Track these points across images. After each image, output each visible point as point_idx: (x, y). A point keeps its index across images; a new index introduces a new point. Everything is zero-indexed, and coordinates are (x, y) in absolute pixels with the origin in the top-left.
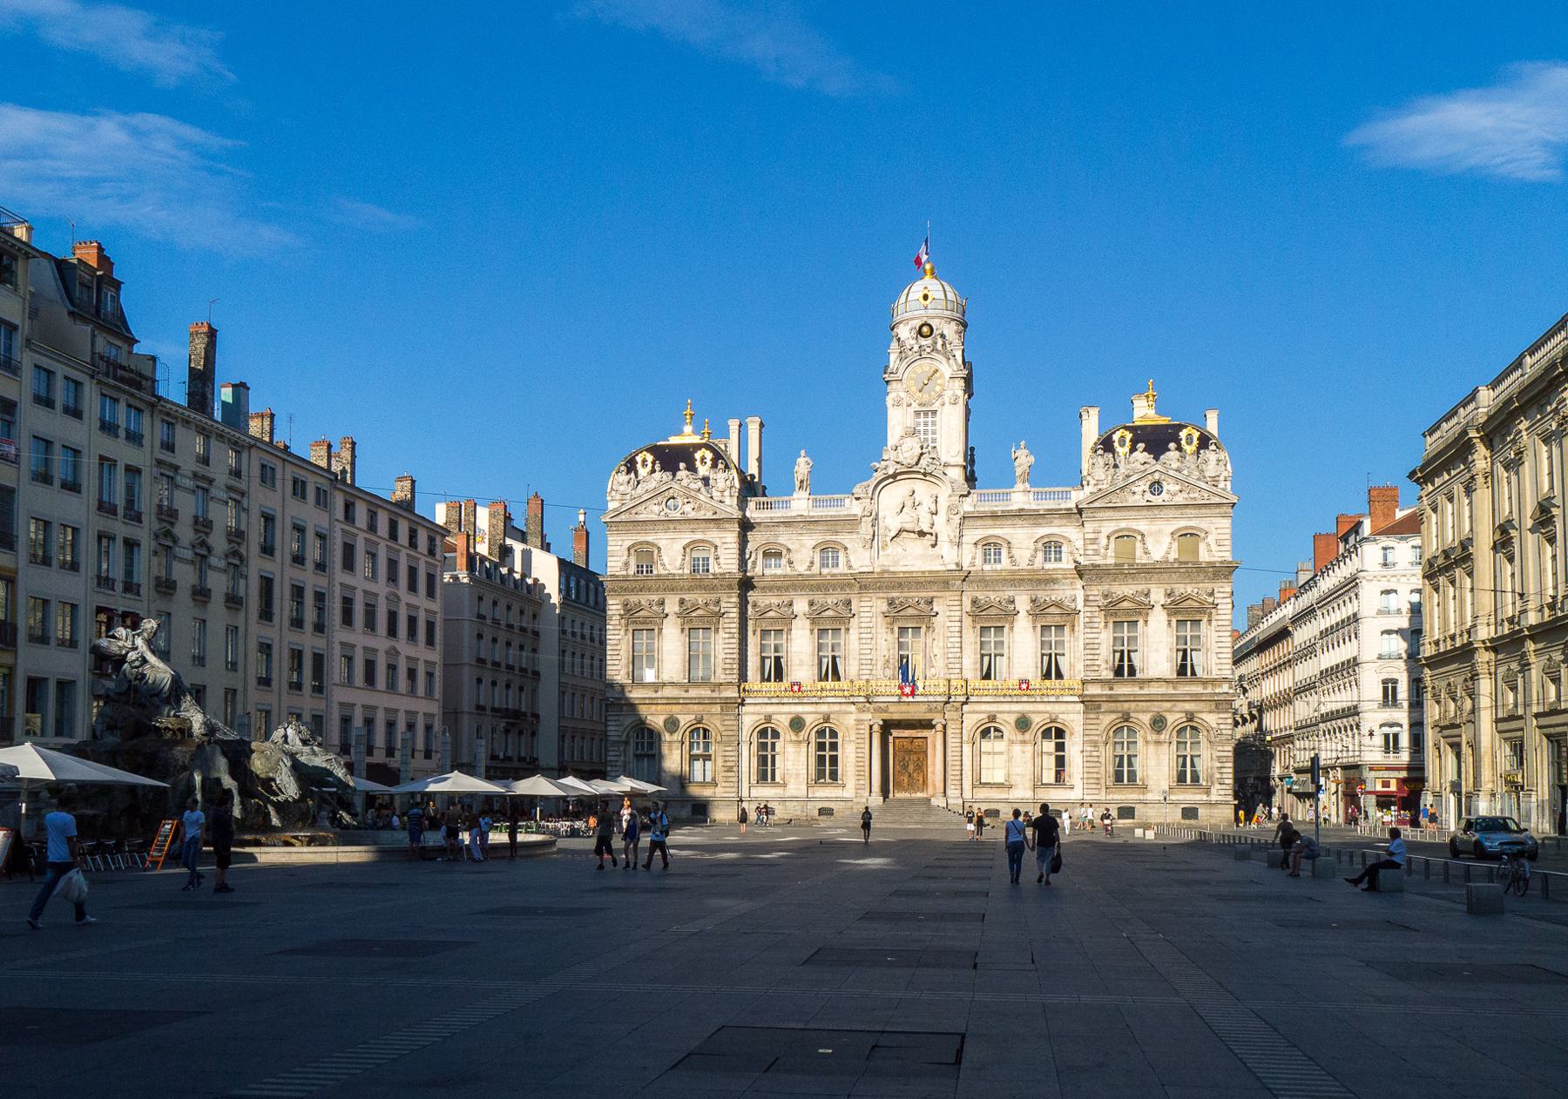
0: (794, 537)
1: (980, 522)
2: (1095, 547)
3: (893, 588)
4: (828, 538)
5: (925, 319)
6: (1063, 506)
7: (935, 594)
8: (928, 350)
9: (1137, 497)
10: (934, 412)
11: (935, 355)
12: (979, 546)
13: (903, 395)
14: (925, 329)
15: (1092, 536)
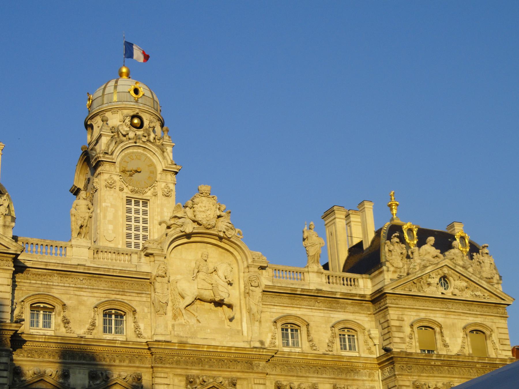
0: (71, 291)
1: (277, 300)
2: (401, 335)
3: (193, 364)
4: (113, 297)
5: (137, 111)
6: (354, 292)
7: (239, 375)
8: (144, 139)
9: (433, 288)
10: (145, 203)
11: (149, 146)
12: (279, 324)
13: (116, 178)
14: (136, 121)
15: (397, 323)
